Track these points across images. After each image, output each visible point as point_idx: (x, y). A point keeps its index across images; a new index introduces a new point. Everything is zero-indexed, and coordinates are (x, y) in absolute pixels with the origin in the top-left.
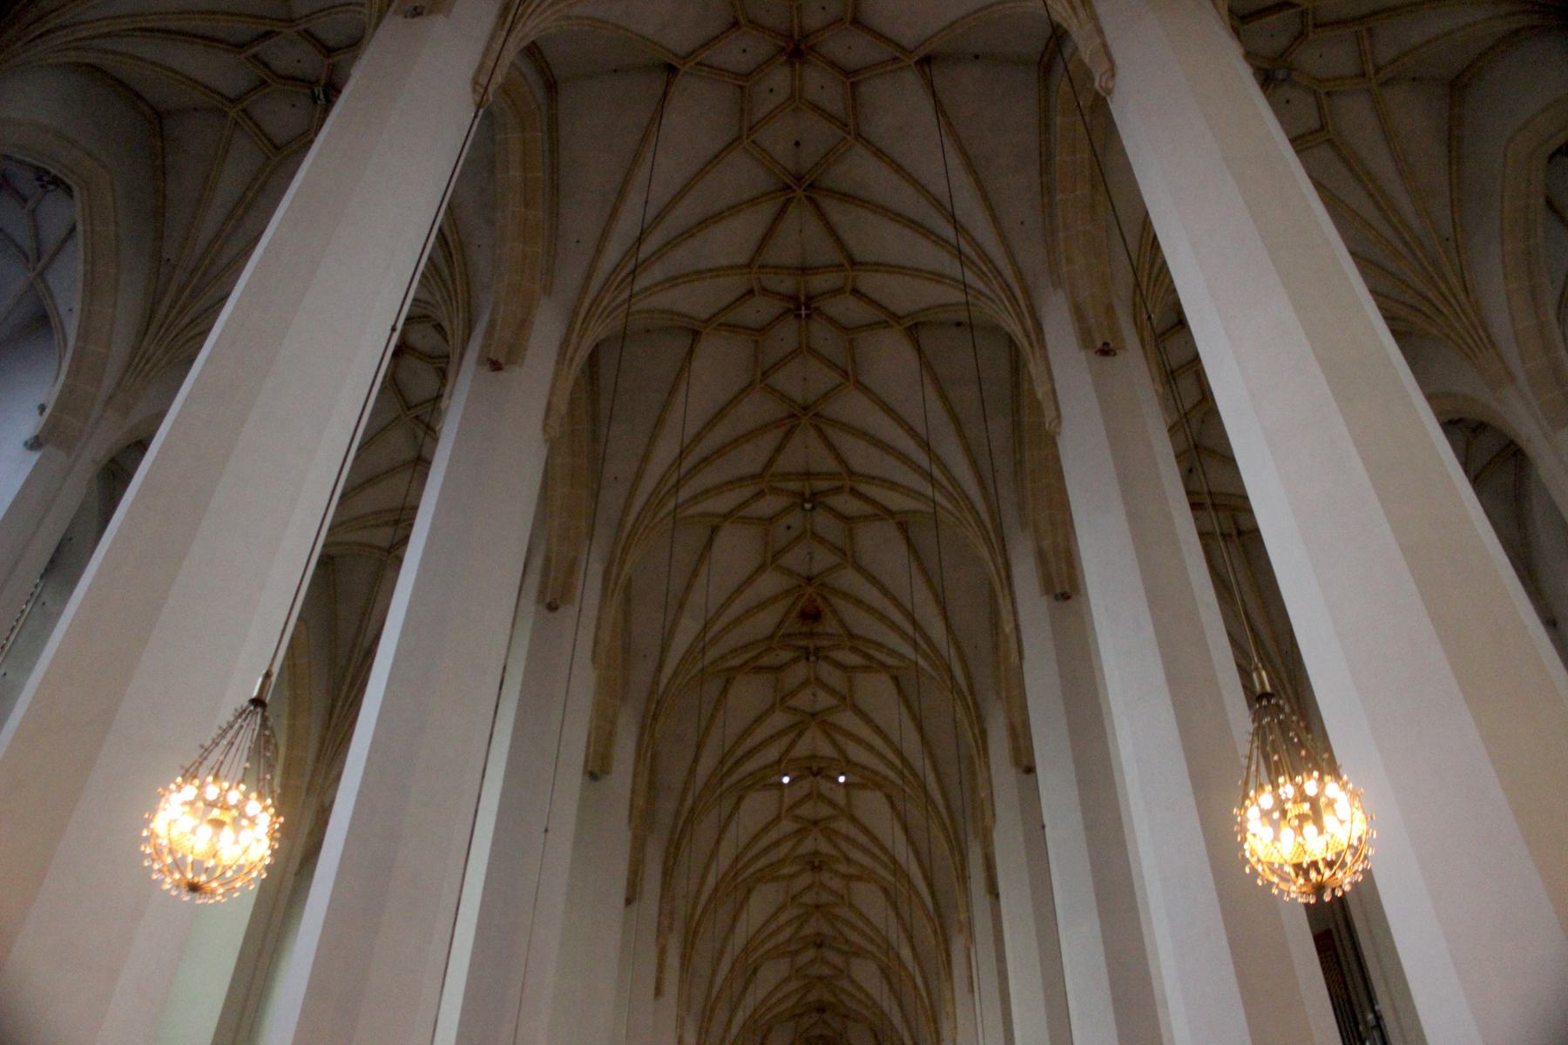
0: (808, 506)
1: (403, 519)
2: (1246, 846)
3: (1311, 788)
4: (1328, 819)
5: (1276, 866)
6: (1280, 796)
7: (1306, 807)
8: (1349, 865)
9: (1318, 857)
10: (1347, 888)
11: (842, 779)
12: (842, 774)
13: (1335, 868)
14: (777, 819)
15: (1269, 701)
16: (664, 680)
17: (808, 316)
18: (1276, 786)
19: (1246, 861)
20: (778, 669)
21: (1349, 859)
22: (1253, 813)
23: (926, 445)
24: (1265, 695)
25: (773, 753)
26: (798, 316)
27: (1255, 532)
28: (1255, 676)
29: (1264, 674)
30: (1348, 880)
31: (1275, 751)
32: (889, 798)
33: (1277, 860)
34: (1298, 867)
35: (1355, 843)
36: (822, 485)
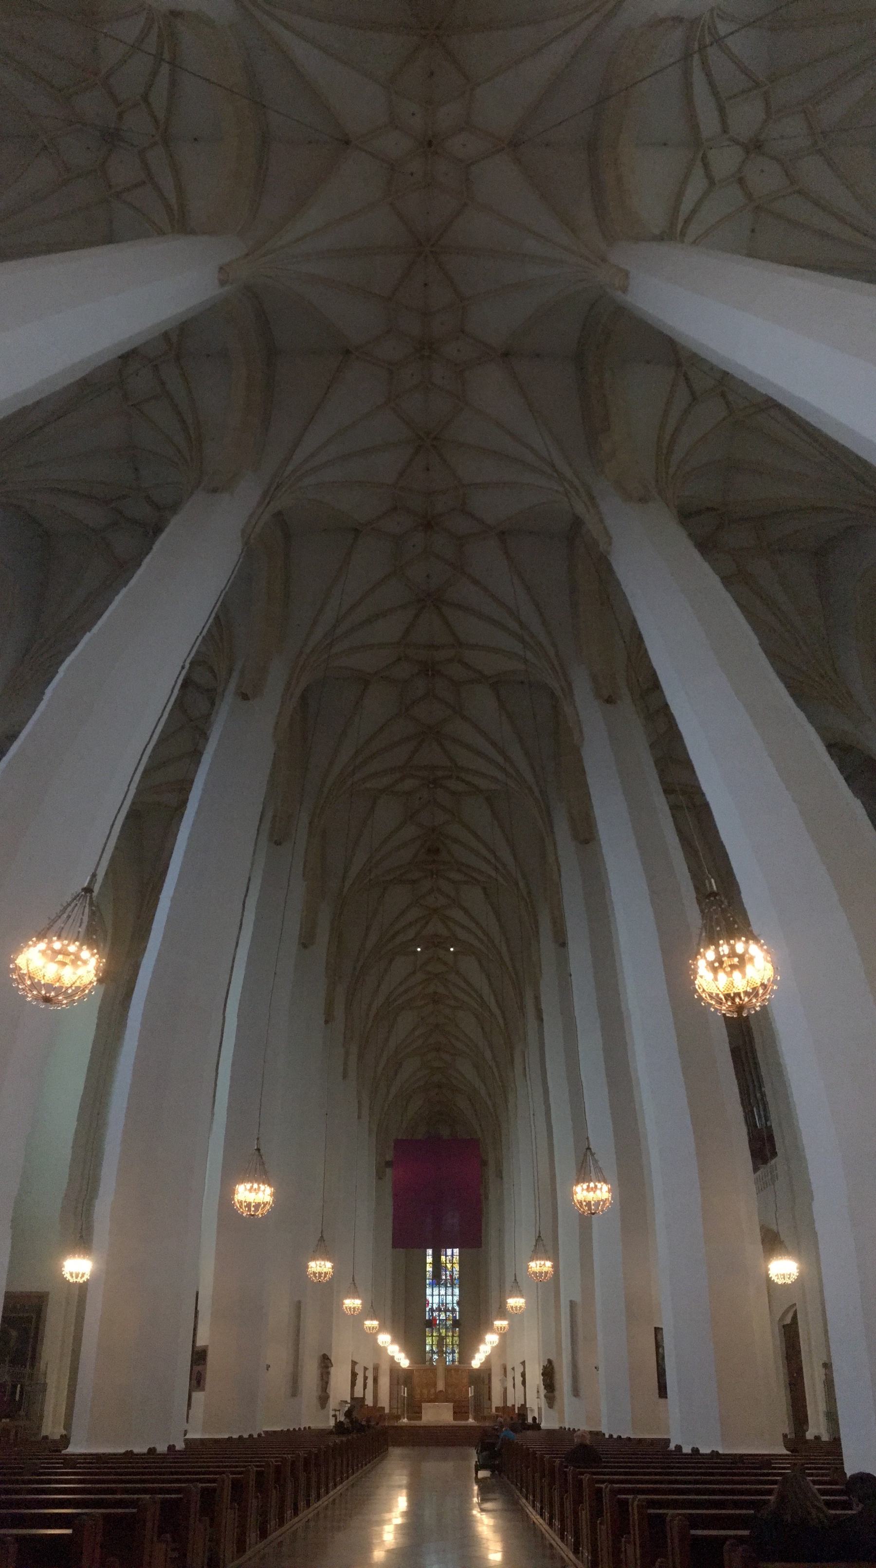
0: (431, 786)
1: (184, 787)
2: (696, 982)
3: (740, 947)
4: (749, 968)
5: (714, 995)
6: (719, 952)
7: (736, 960)
8: (760, 995)
9: (741, 991)
10: (758, 1009)
11: (452, 949)
12: (452, 947)
13: (751, 996)
14: (414, 972)
15: (715, 898)
16: (345, 890)
17: (433, 675)
18: (717, 946)
19: (696, 991)
20: (413, 882)
21: (761, 991)
22: (701, 964)
23: (493, 852)
24: (713, 894)
25: (411, 933)
26: (428, 675)
27: (706, 806)
28: (707, 881)
29: (713, 881)
30: (758, 1004)
31: (718, 924)
32: (480, 962)
33: (715, 991)
34: (727, 996)
35: (766, 982)
36: (440, 773)
